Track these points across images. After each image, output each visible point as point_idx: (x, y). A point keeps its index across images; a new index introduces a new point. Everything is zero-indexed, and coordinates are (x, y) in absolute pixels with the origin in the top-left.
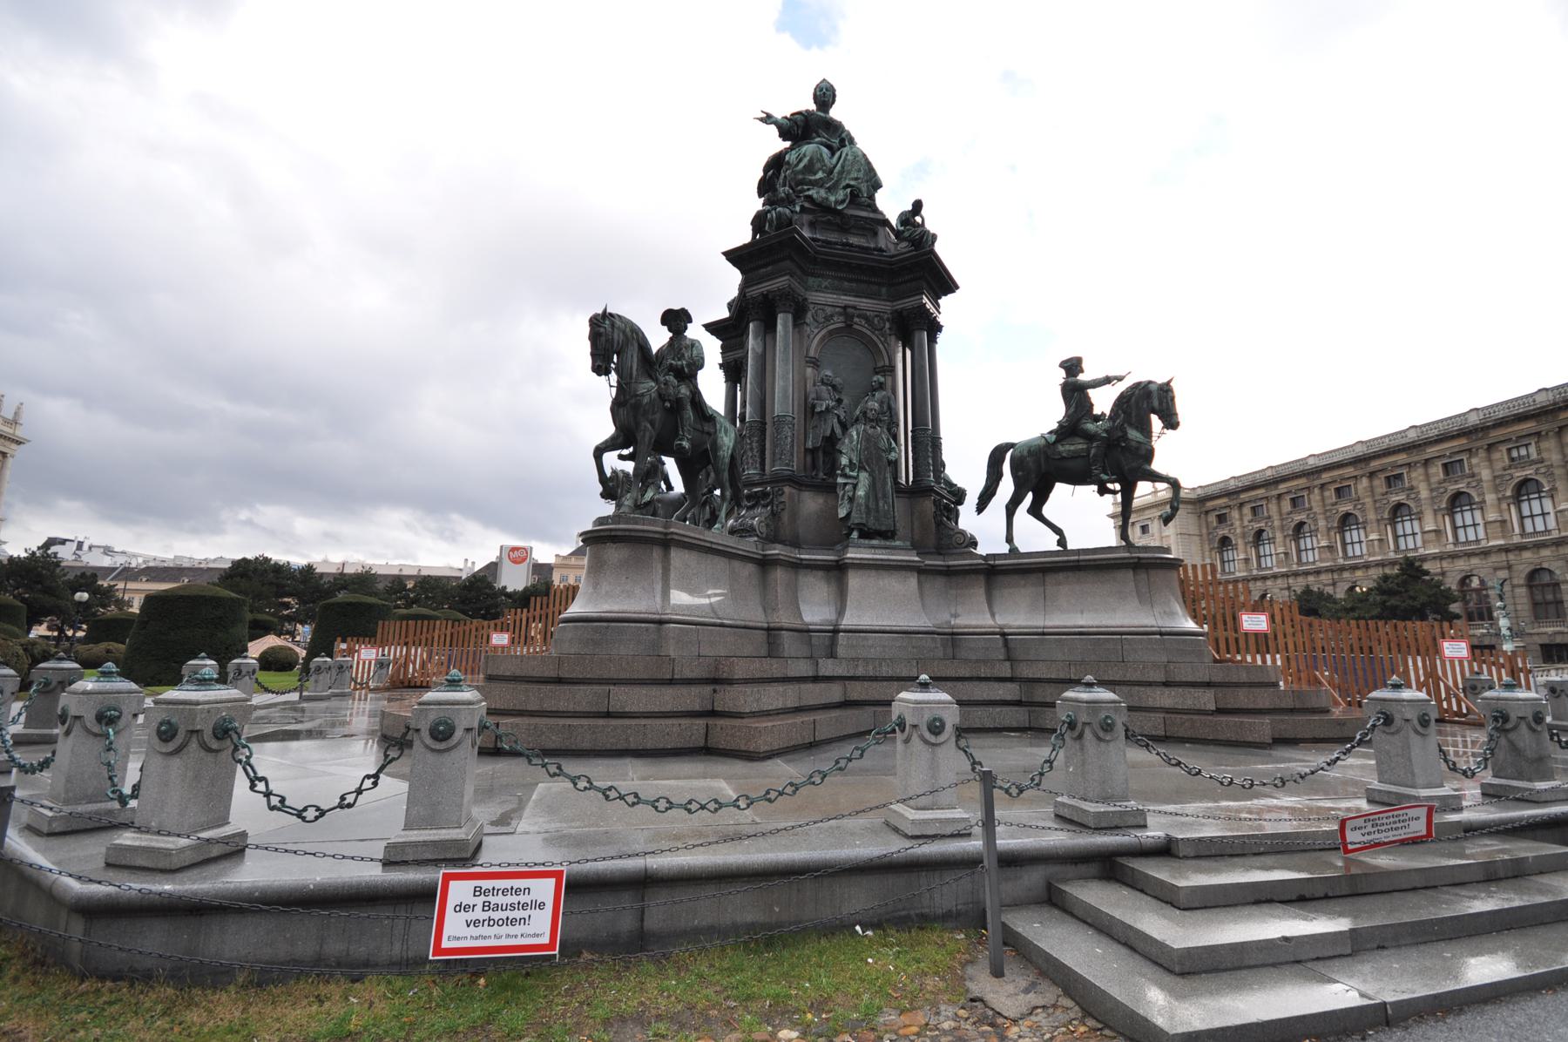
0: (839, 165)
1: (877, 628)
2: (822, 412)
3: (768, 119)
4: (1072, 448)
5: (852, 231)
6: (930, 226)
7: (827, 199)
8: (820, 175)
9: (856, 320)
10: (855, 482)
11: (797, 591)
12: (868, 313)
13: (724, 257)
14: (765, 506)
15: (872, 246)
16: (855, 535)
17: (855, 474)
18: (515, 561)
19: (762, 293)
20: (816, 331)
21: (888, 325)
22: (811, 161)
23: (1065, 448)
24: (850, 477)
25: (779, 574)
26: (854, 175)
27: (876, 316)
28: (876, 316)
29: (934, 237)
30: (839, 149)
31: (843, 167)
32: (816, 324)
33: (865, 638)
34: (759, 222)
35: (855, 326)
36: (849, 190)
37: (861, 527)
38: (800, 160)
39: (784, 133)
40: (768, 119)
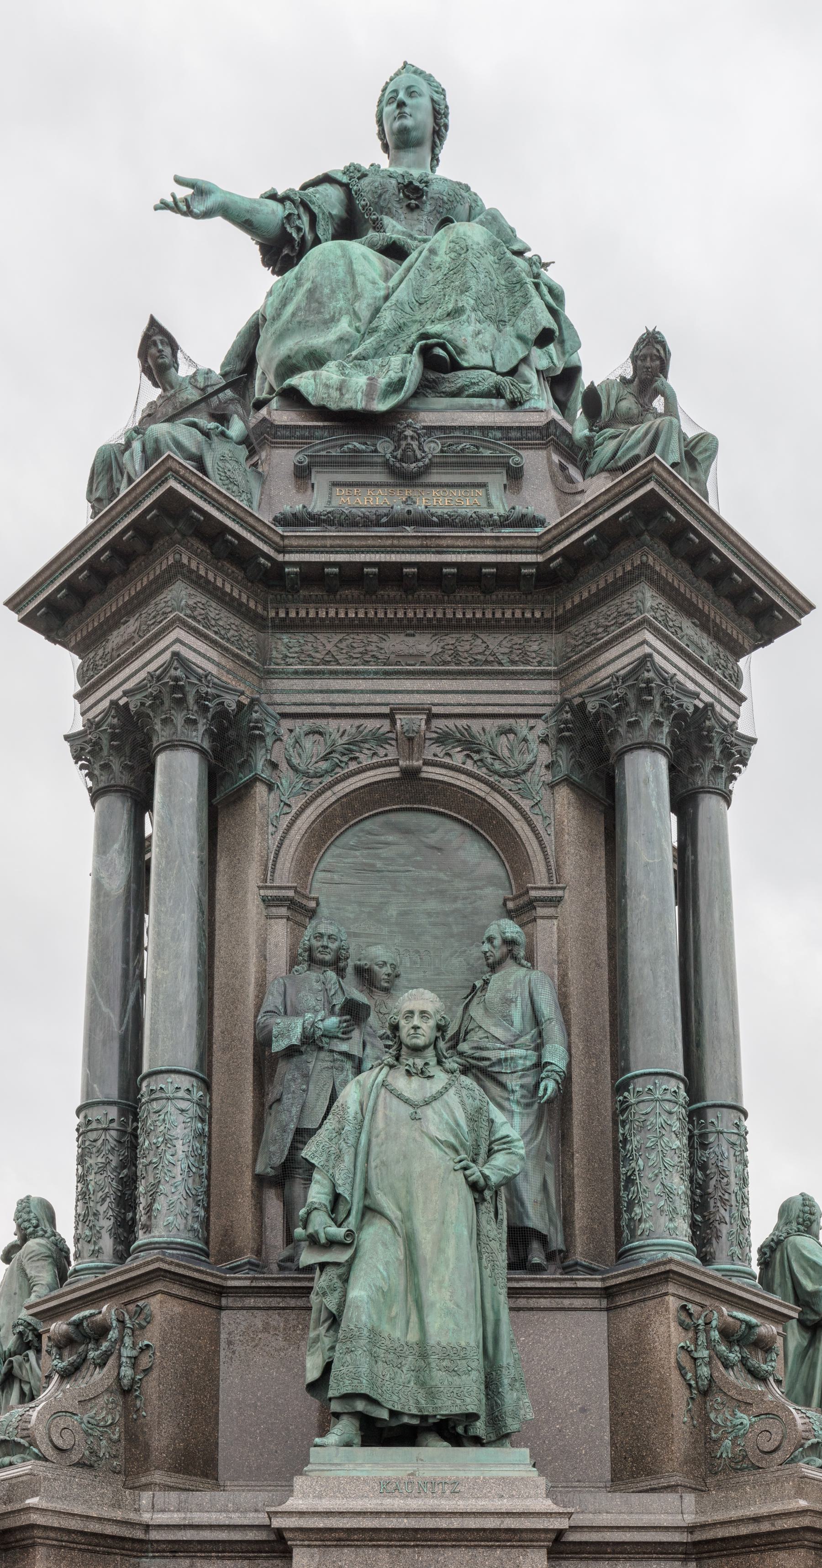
2: (292, 1052)
8: (344, 326)
9: (432, 751)
12: (476, 725)
13: (15, 617)
19: (114, 703)
21: (544, 755)
24: (332, 1243)
35: (432, 773)
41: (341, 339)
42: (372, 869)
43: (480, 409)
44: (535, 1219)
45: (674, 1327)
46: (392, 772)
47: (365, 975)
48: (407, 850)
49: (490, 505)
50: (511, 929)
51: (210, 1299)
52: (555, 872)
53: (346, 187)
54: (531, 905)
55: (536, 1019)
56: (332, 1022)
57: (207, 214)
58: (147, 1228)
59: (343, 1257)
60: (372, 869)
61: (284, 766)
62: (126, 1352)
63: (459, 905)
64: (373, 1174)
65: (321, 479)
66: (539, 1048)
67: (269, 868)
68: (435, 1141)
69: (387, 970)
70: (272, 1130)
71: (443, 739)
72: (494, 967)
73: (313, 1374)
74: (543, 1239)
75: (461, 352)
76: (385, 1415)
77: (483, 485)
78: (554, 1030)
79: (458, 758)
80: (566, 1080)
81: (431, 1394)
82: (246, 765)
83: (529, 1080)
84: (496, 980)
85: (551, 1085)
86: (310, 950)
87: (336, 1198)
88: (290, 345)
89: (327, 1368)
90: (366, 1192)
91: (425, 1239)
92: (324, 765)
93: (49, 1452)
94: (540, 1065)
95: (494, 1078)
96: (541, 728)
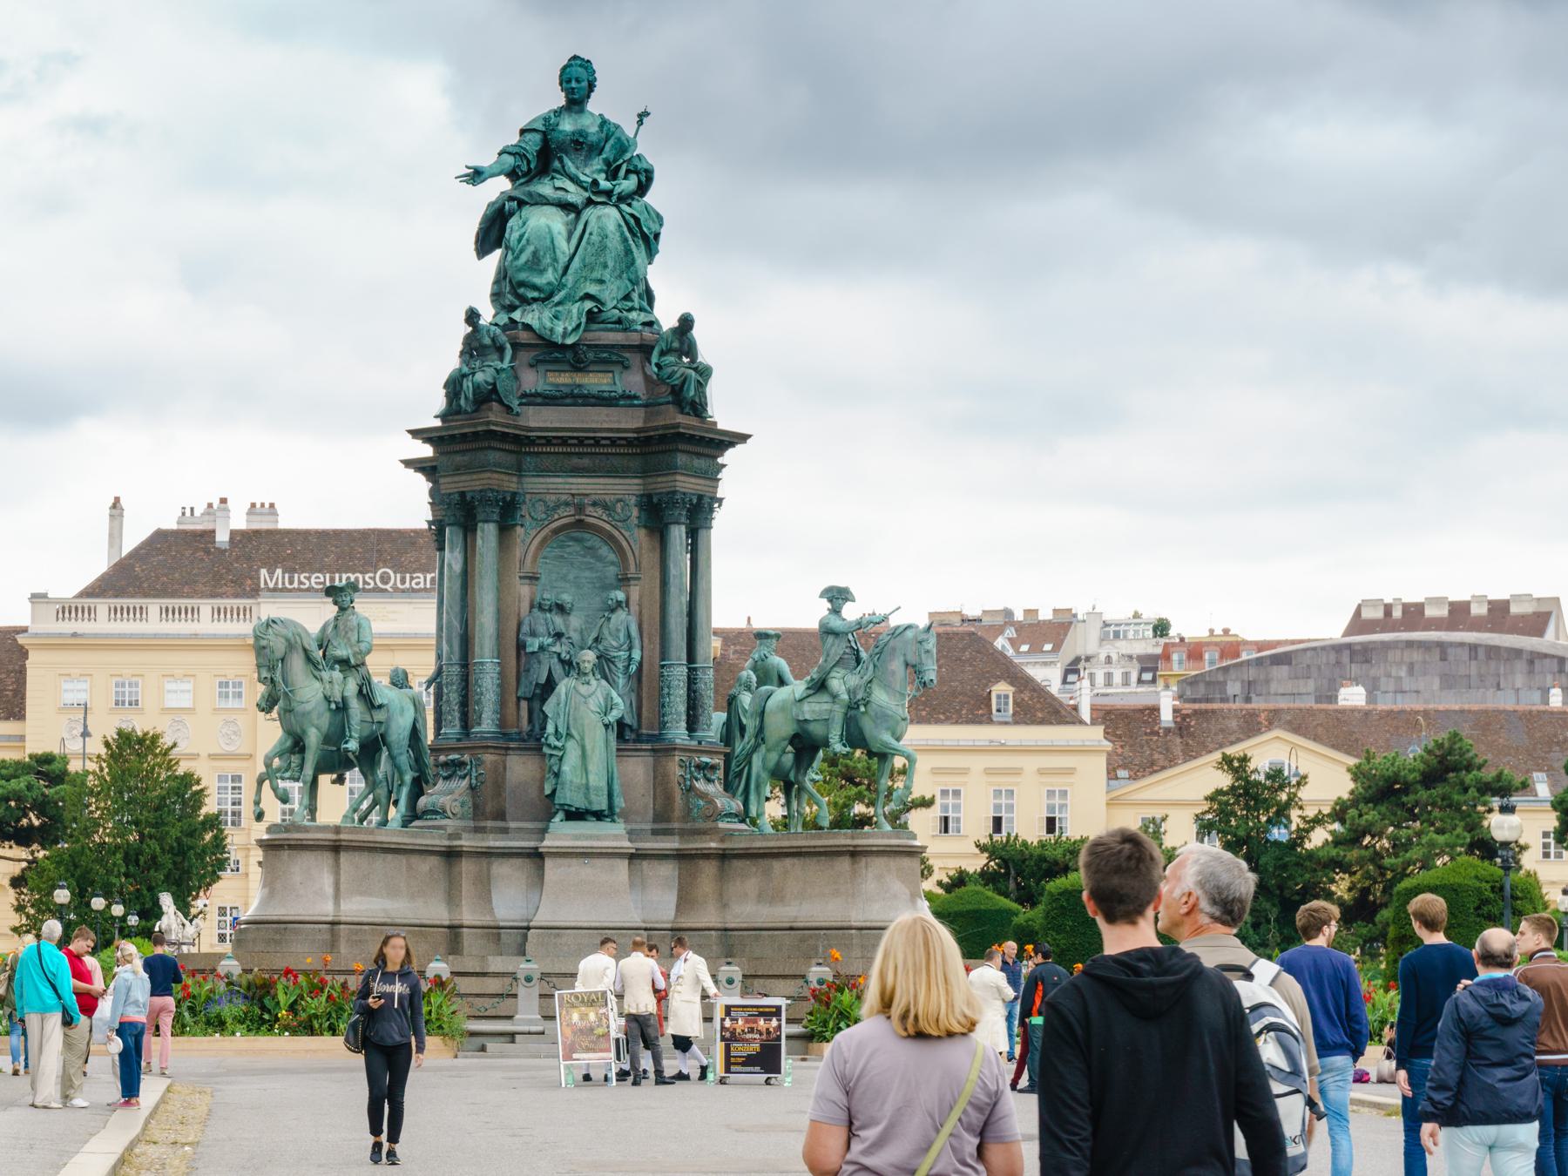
0: (577, 259)
1: (573, 924)
2: (533, 653)
3: (476, 176)
4: (817, 707)
5: (591, 368)
6: (705, 355)
7: (552, 330)
8: (550, 276)
10: (560, 754)
11: (489, 884)
13: (410, 436)
14: (464, 777)
15: (620, 391)
16: (560, 815)
17: (559, 744)
20: (533, 533)
21: (635, 512)
22: (535, 253)
24: (556, 748)
25: (466, 867)
26: (596, 275)
27: (619, 501)
28: (619, 501)
29: (705, 372)
30: (590, 202)
31: (583, 260)
32: (534, 524)
34: (454, 386)
36: (589, 305)
37: (566, 807)
38: (521, 251)
39: (512, 175)
40: (476, 176)
41: (549, 284)
42: (562, 557)
43: (611, 330)
44: (628, 721)
45: (677, 768)
46: (571, 519)
47: (561, 609)
48: (578, 549)
49: (615, 384)
50: (620, 596)
51: (503, 752)
52: (638, 566)
53: (544, 133)
54: (628, 579)
56: (550, 640)
58: (479, 724)
59: (560, 754)
60: (562, 557)
61: (527, 516)
62: (474, 774)
63: (598, 574)
64: (571, 722)
65: (542, 368)
66: (630, 649)
67: (522, 562)
68: (592, 711)
69: (569, 606)
72: (613, 611)
73: (548, 791)
74: (630, 727)
75: (603, 304)
76: (574, 809)
77: (612, 372)
78: (637, 643)
79: (600, 511)
80: (641, 664)
81: (590, 803)
82: (513, 517)
83: (626, 664)
84: (614, 617)
85: (635, 668)
86: (540, 604)
87: (557, 730)
88: (523, 276)
89: (554, 791)
90: (568, 728)
91: (588, 748)
92: (544, 516)
93: (451, 815)
94: (630, 658)
95: (613, 663)
96: (633, 500)
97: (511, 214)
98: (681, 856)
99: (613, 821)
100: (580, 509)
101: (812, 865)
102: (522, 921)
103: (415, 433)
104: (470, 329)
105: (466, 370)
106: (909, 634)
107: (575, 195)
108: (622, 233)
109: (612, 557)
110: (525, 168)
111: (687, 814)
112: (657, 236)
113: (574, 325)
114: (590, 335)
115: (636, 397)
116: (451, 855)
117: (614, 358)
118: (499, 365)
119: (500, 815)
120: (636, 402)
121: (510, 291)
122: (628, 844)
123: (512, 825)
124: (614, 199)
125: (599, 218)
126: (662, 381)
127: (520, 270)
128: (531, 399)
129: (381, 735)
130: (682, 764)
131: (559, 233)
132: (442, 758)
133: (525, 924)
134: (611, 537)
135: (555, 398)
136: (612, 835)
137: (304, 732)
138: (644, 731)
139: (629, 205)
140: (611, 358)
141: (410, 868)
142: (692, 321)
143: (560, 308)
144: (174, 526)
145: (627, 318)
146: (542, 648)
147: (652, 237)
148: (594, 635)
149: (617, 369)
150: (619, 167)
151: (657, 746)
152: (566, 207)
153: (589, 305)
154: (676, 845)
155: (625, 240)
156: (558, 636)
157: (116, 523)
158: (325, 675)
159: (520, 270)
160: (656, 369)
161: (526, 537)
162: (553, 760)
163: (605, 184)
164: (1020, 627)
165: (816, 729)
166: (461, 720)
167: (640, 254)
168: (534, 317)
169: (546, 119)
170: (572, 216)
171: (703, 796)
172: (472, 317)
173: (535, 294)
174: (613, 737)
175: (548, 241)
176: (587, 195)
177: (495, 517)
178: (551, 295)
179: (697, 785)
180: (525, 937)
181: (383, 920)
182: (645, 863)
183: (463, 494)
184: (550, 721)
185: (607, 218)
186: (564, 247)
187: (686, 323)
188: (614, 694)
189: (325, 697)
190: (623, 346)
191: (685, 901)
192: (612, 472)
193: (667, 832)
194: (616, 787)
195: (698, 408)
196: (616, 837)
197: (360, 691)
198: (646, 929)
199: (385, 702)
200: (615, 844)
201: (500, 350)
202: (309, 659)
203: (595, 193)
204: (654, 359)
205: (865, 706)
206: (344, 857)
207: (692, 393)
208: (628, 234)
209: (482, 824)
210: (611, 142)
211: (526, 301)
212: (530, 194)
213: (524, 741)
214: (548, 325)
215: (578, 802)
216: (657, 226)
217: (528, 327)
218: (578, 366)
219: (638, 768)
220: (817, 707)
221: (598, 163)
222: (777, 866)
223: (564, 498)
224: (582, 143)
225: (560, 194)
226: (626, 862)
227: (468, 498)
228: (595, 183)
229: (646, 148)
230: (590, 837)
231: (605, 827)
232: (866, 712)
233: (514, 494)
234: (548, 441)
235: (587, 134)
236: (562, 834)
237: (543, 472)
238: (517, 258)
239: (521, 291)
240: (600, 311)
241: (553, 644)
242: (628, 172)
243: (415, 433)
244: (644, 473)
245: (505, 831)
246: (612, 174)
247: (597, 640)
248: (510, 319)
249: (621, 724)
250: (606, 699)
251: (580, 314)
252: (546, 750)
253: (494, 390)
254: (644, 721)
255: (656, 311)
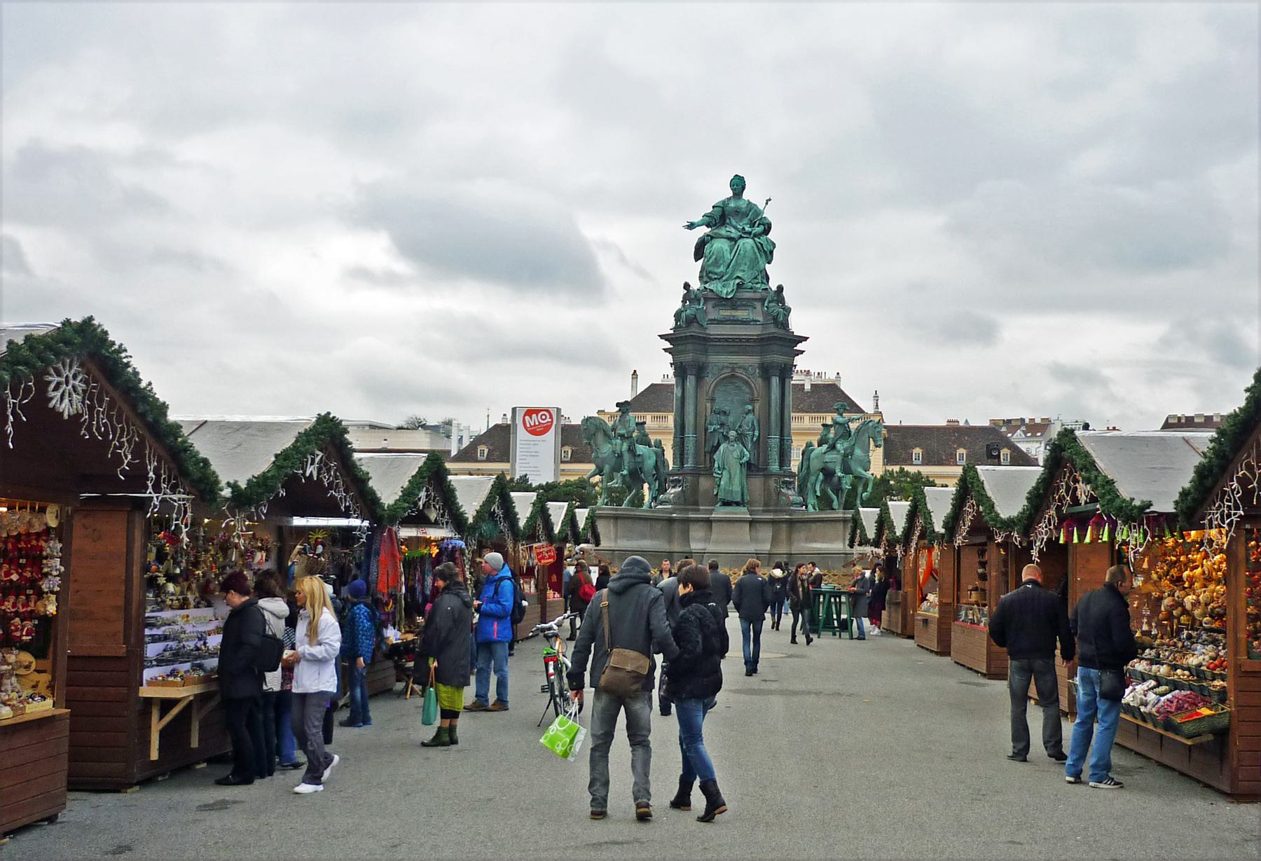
3: (691, 226)
6: (788, 303)
9: (737, 370)
13: (659, 338)
14: (680, 487)
17: (720, 472)
18: (537, 431)
21: (757, 371)
23: (828, 457)
24: (718, 474)
26: (742, 268)
28: (750, 366)
30: (741, 237)
31: (736, 261)
33: (718, 556)
34: (678, 316)
36: (738, 281)
38: (710, 258)
40: (691, 226)
41: (722, 272)
43: (748, 292)
44: (752, 462)
46: (730, 374)
47: (725, 413)
50: (750, 407)
55: (753, 424)
57: (695, 228)
65: (717, 308)
66: (754, 431)
67: (707, 393)
70: (707, 445)
71: (740, 367)
72: (747, 414)
73: (715, 493)
76: (726, 501)
79: (742, 370)
84: (747, 417)
87: (719, 467)
89: (717, 494)
91: (732, 474)
94: (754, 435)
96: (757, 365)
97: (708, 242)
98: (773, 522)
99: (744, 506)
100: (733, 369)
101: (828, 525)
102: (702, 550)
103: (661, 337)
104: (686, 292)
105: (683, 309)
106: (871, 424)
107: (734, 234)
108: (754, 250)
109: (747, 390)
110: (714, 223)
111: (777, 504)
112: (771, 252)
113: (731, 289)
114: (738, 294)
115: (759, 321)
116: (671, 521)
117: (749, 304)
118: (698, 307)
119: (696, 503)
120: (758, 323)
121: (705, 276)
122: (749, 516)
123: (701, 508)
124: (752, 236)
125: (744, 243)
126: (770, 314)
127: (709, 266)
128: (713, 321)
129: (640, 468)
130: (776, 483)
131: (727, 250)
132: (671, 478)
133: (703, 551)
134: (747, 381)
135: (722, 321)
136: (742, 513)
137: (603, 467)
138: (760, 467)
139: (759, 238)
140: (748, 304)
141: (651, 526)
142: (783, 289)
143: (725, 282)
144: (660, 382)
145: (755, 287)
146: (714, 429)
147: (768, 252)
148: (739, 424)
149: (751, 309)
150: (755, 222)
151: (765, 473)
152: (730, 239)
153: (738, 281)
154: (772, 517)
155: (756, 253)
156: (722, 425)
157: (635, 381)
158: (614, 442)
159: (709, 266)
160: (766, 309)
161: (710, 380)
162: (717, 479)
163: (748, 229)
164: (1027, 425)
165: (831, 466)
166: (680, 461)
167: (762, 261)
168: (715, 286)
169: (724, 202)
170: (733, 243)
171: (785, 495)
172: (687, 286)
173: (716, 276)
174: (744, 470)
175: (721, 254)
176: (740, 234)
177: (694, 373)
178: (723, 276)
179: (783, 490)
180: (703, 556)
181: (637, 549)
182: (757, 524)
183: (682, 363)
184: (716, 462)
185: (748, 243)
186: (728, 256)
187: (780, 289)
188: (744, 449)
189: (613, 451)
190: (753, 299)
191: (774, 541)
192: (745, 353)
193: (769, 511)
194: (745, 491)
195: (785, 325)
196: (744, 513)
197: (629, 448)
198: (756, 554)
199: (641, 453)
200: (745, 516)
201: (699, 300)
202: (606, 434)
203: (745, 233)
204: (766, 304)
205: (851, 455)
206: (619, 521)
207: (781, 319)
208: (756, 251)
209: (688, 507)
210: (752, 211)
211: (711, 279)
212: (716, 234)
213: (707, 470)
214: (720, 289)
215: (729, 499)
216: (772, 247)
217: (711, 290)
218: (734, 307)
219: (757, 482)
220: (831, 456)
221: (746, 220)
222: (813, 526)
223: (726, 364)
224: (738, 212)
225: (728, 233)
226: (748, 524)
227: (684, 364)
228: (744, 228)
229: (768, 214)
230: (733, 513)
231: (742, 509)
232: (851, 458)
233: (703, 363)
234: (719, 340)
235: (741, 208)
236: (720, 513)
237: (718, 353)
238: (708, 261)
239: (710, 275)
240: (743, 284)
241: (720, 428)
242: (759, 224)
243: (661, 337)
244: (761, 354)
245: (698, 510)
246: (752, 225)
247: (740, 427)
248: (705, 287)
249: (749, 464)
250: (741, 452)
251: (734, 283)
252: (714, 475)
253: (695, 318)
254: (760, 463)
255: (770, 284)
